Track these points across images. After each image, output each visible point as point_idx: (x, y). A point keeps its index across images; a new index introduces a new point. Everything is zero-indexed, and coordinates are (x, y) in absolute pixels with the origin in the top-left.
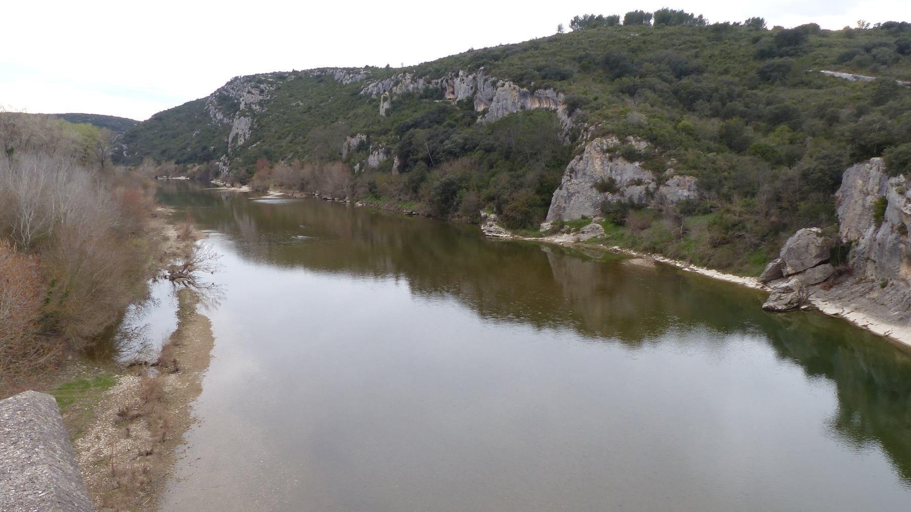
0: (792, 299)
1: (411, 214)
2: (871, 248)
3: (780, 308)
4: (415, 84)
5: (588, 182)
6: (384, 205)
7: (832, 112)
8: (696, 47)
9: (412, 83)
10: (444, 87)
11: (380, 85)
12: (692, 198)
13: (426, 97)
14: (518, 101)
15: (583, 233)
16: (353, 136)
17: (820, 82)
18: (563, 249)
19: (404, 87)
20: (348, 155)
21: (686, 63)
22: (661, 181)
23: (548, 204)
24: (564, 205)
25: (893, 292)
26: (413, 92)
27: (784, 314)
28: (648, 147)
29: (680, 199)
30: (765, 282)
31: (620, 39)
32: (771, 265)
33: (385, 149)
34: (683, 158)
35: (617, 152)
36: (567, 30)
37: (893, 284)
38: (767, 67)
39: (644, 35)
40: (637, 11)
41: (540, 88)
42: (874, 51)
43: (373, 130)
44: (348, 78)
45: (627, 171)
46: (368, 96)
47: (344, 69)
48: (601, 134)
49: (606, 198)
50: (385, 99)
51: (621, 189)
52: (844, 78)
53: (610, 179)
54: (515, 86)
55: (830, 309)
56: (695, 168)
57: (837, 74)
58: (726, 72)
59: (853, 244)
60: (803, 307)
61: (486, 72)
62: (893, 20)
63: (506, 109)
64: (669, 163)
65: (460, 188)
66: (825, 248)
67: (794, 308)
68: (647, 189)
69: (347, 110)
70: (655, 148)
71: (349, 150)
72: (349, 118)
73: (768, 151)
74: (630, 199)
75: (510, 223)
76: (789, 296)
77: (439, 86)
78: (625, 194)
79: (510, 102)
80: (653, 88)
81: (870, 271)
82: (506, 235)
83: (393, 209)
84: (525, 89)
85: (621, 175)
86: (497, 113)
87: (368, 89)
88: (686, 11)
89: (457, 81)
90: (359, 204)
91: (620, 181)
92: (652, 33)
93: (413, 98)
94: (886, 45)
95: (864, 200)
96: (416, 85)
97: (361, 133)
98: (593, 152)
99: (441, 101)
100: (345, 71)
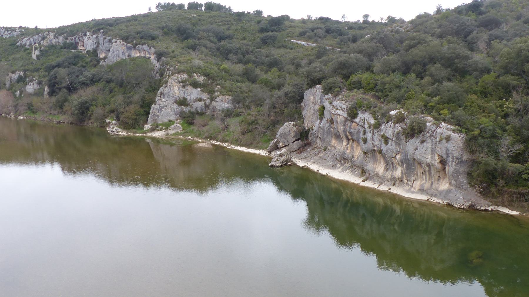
0: (283, 160)
1: (59, 123)
2: (318, 131)
3: (278, 165)
4: (57, 39)
5: (171, 100)
6: (39, 118)
7: (298, 62)
8: (228, 24)
9: (54, 39)
10: (77, 42)
11: (31, 39)
12: (230, 108)
13: (65, 48)
14: (126, 52)
15: (170, 130)
16: (13, 72)
17: (291, 46)
18: (159, 140)
19: (49, 41)
20: (11, 85)
21: (223, 33)
22: (212, 99)
23: (148, 113)
24: (157, 114)
25: (329, 153)
26: (56, 44)
27: (280, 168)
28: (204, 79)
29: (223, 109)
30: (270, 152)
31: (186, 18)
32: (272, 142)
33: (38, 81)
34: (224, 86)
35: (187, 83)
36: (154, 10)
37: (329, 149)
38: (265, 37)
39: (199, 16)
40: (194, 2)
41: (139, 44)
42: (315, 31)
43: (28, 69)
44: (7, 34)
45: (194, 94)
46: (23, 46)
47: (3, 27)
48: (177, 72)
49: (182, 109)
50: (36, 49)
51: (191, 104)
52: (302, 44)
53: (184, 98)
54: (123, 42)
55: (301, 163)
56: (230, 91)
57: (299, 42)
58: (244, 39)
59: (311, 129)
60: (289, 164)
61: (105, 33)
62: (323, 16)
63: (119, 56)
64: (217, 89)
65: (91, 105)
66: (298, 133)
67: (285, 164)
68: (205, 103)
69: (7, 55)
70: (209, 80)
71: (11, 82)
72: (10, 60)
73: (268, 82)
74: (196, 109)
75: (125, 126)
76: (282, 159)
77: (73, 41)
78: (193, 107)
79: (121, 53)
80: (205, 46)
81: (319, 143)
82: (123, 133)
83: (46, 120)
84: (130, 45)
85: (190, 95)
86: (113, 59)
87: (23, 42)
88: (221, 4)
89: (86, 38)
90: (21, 118)
91: (190, 100)
92: (203, 15)
93: (56, 48)
94: (320, 28)
95: (314, 107)
96: (57, 40)
97: (20, 70)
98: (173, 82)
99: (75, 51)
100: (4, 29)
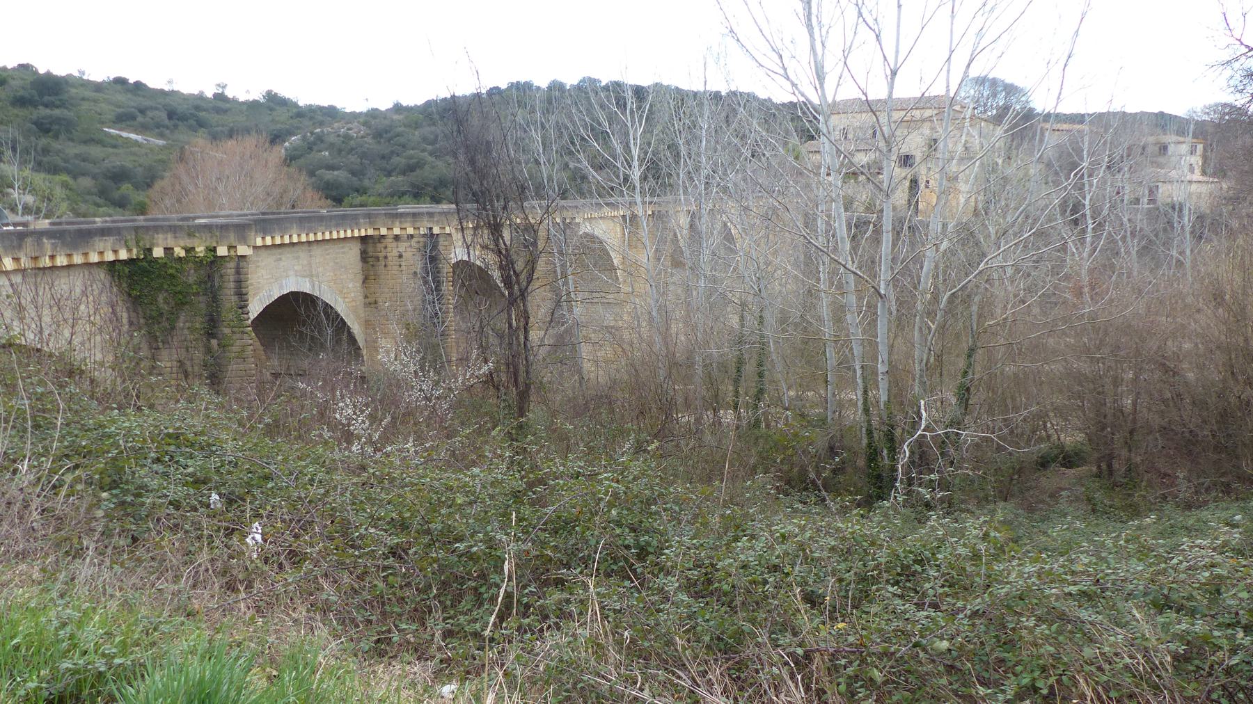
57: (125, 134)
